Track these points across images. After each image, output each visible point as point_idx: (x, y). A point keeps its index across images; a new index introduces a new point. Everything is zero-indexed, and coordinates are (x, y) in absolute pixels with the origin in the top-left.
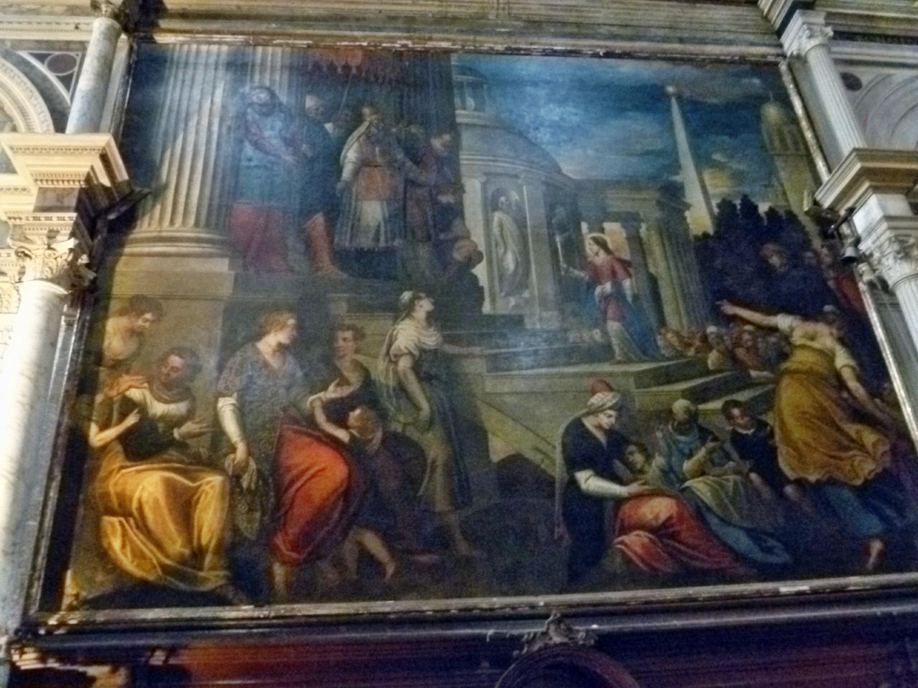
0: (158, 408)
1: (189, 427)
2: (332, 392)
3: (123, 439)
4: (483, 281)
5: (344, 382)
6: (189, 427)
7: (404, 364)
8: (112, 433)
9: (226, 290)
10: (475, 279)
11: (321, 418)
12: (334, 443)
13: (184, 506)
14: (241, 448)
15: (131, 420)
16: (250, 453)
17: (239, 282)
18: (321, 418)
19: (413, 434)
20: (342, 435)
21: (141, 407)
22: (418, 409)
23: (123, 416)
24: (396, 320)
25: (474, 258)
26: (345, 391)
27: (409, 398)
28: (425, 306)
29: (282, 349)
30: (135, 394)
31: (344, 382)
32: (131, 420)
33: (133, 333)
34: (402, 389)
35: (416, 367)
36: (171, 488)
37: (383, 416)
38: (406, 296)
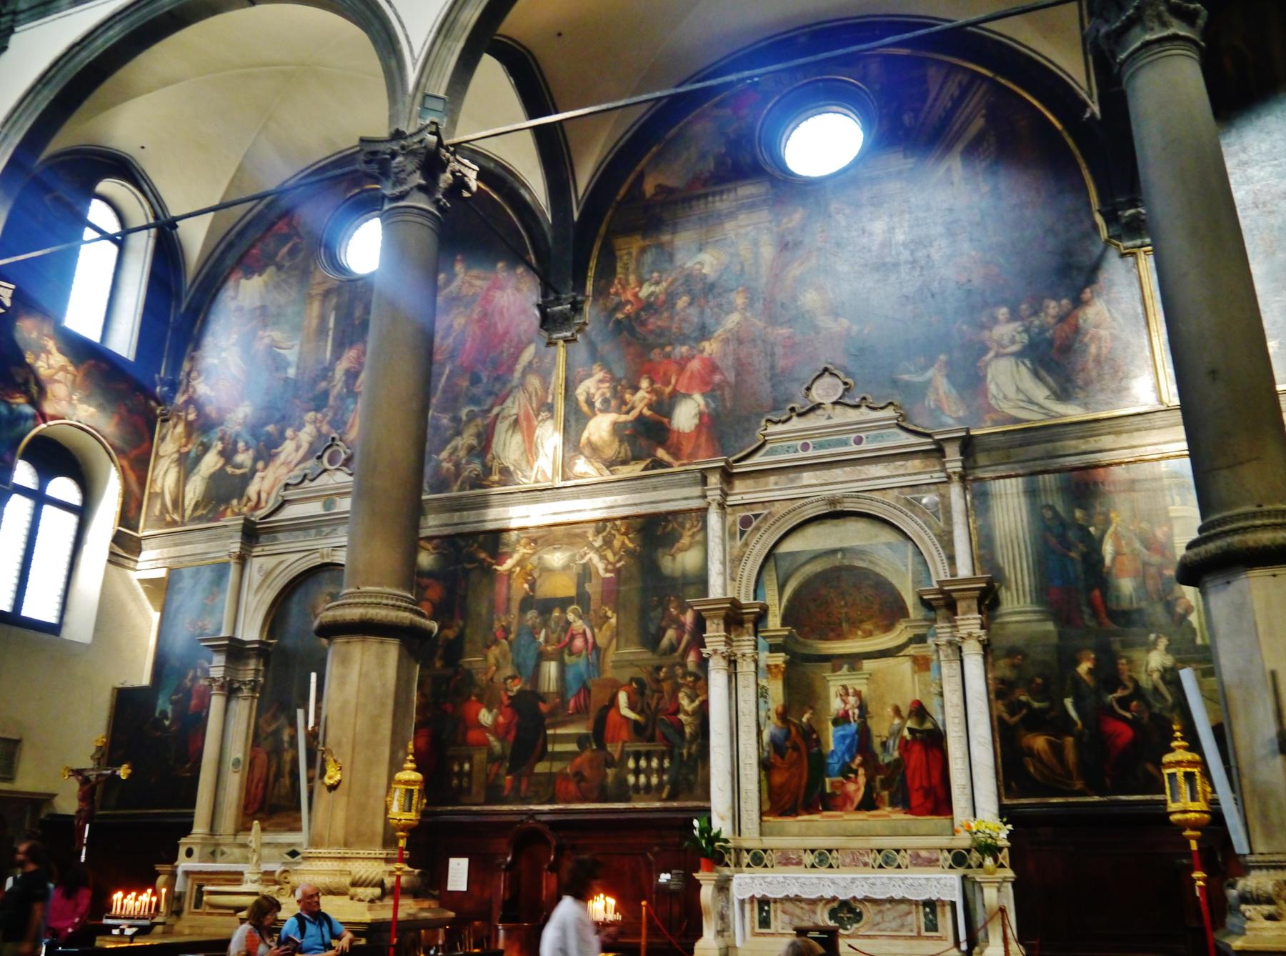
0: (1036, 705)
1: (1052, 714)
2: (1119, 693)
3: (1023, 720)
4: (1196, 624)
5: (1125, 687)
6: (1052, 714)
7: (1156, 676)
8: (1016, 719)
9: (1054, 639)
10: (1190, 624)
11: (1117, 707)
12: (1124, 719)
13: (1057, 750)
14: (1079, 723)
15: (1024, 712)
16: (1084, 725)
17: (1061, 635)
18: (1117, 707)
19: (1167, 714)
20: (1128, 715)
21: (1027, 705)
22: (1166, 700)
23: (1021, 709)
24: (1148, 651)
25: (1189, 610)
26: (1126, 693)
27: (1162, 696)
28: (1163, 642)
29: (1090, 671)
30: (1023, 698)
31: (1125, 687)
32: (1024, 712)
33: (1014, 666)
34: (1156, 689)
35: (1163, 678)
36: (1050, 743)
37: (1149, 706)
38: (1152, 636)
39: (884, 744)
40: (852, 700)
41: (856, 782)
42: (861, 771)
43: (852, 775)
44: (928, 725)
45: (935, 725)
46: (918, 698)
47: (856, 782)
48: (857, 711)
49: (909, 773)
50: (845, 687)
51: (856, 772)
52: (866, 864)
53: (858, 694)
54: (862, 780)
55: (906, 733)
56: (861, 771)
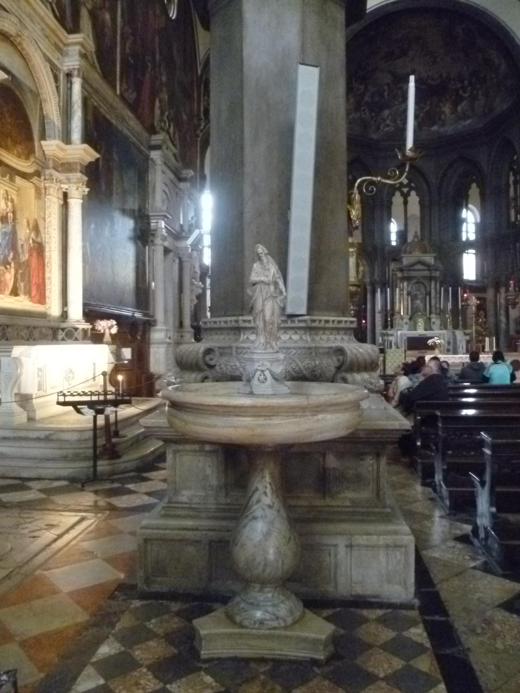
39: (22, 245)
40: (10, 204)
41: (10, 272)
42: (13, 265)
43: (8, 266)
44: (39, 240)
45: (42, 240)
46: (36, 218)
47: (10, 272)
48: (12, 215)
49: (31, 272)
50: (7, 191)
51: (9, 264)
52: (22, 338)
53: (12, 201)
54: (13, 271)
55: (31, 241)
56: (13, 265)
